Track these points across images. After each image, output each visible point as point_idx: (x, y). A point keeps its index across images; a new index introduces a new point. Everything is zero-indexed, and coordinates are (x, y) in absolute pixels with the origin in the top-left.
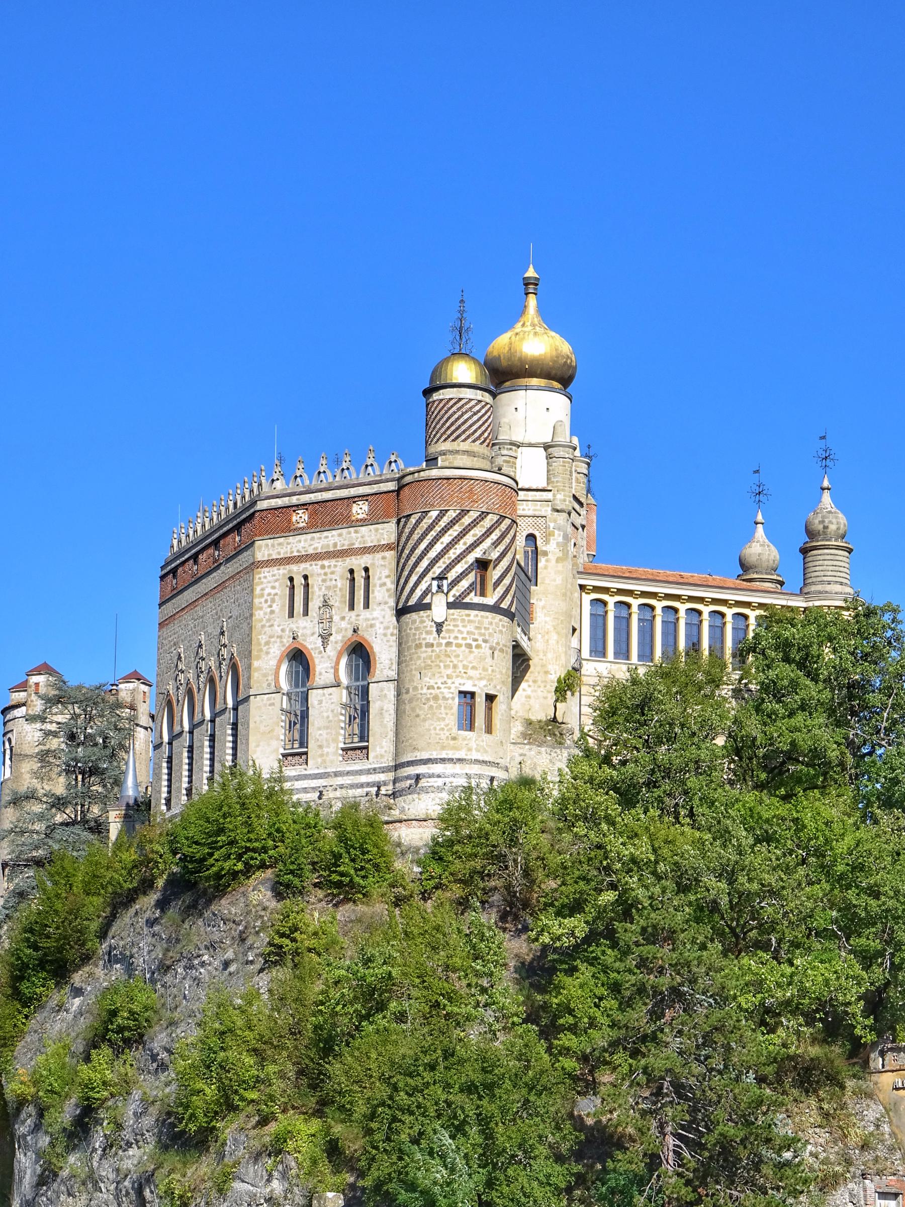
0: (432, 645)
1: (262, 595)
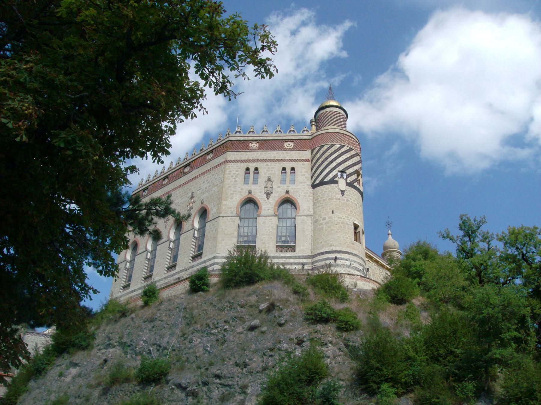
0: (340, 199)
1: (230, 174)
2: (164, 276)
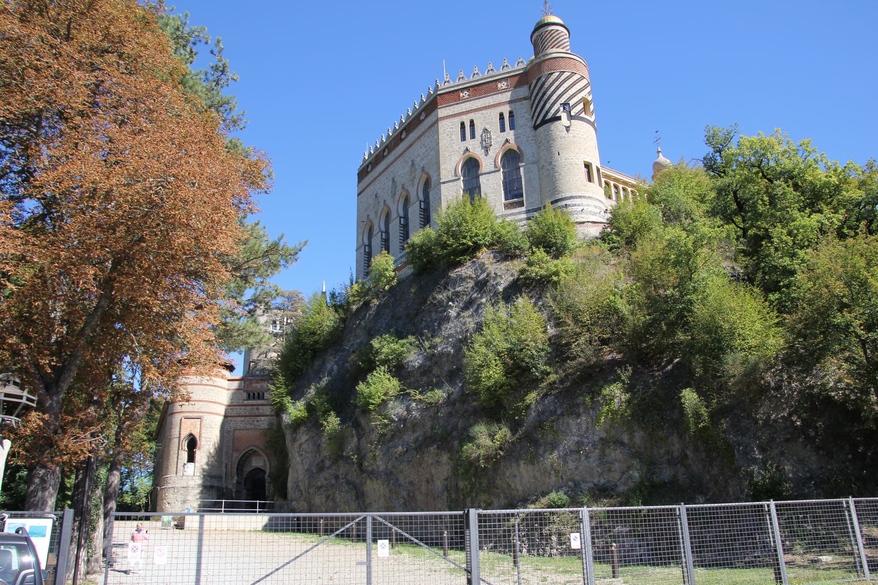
2: (400, 255)
